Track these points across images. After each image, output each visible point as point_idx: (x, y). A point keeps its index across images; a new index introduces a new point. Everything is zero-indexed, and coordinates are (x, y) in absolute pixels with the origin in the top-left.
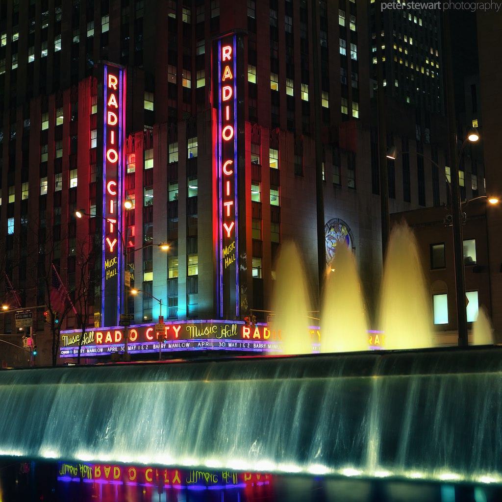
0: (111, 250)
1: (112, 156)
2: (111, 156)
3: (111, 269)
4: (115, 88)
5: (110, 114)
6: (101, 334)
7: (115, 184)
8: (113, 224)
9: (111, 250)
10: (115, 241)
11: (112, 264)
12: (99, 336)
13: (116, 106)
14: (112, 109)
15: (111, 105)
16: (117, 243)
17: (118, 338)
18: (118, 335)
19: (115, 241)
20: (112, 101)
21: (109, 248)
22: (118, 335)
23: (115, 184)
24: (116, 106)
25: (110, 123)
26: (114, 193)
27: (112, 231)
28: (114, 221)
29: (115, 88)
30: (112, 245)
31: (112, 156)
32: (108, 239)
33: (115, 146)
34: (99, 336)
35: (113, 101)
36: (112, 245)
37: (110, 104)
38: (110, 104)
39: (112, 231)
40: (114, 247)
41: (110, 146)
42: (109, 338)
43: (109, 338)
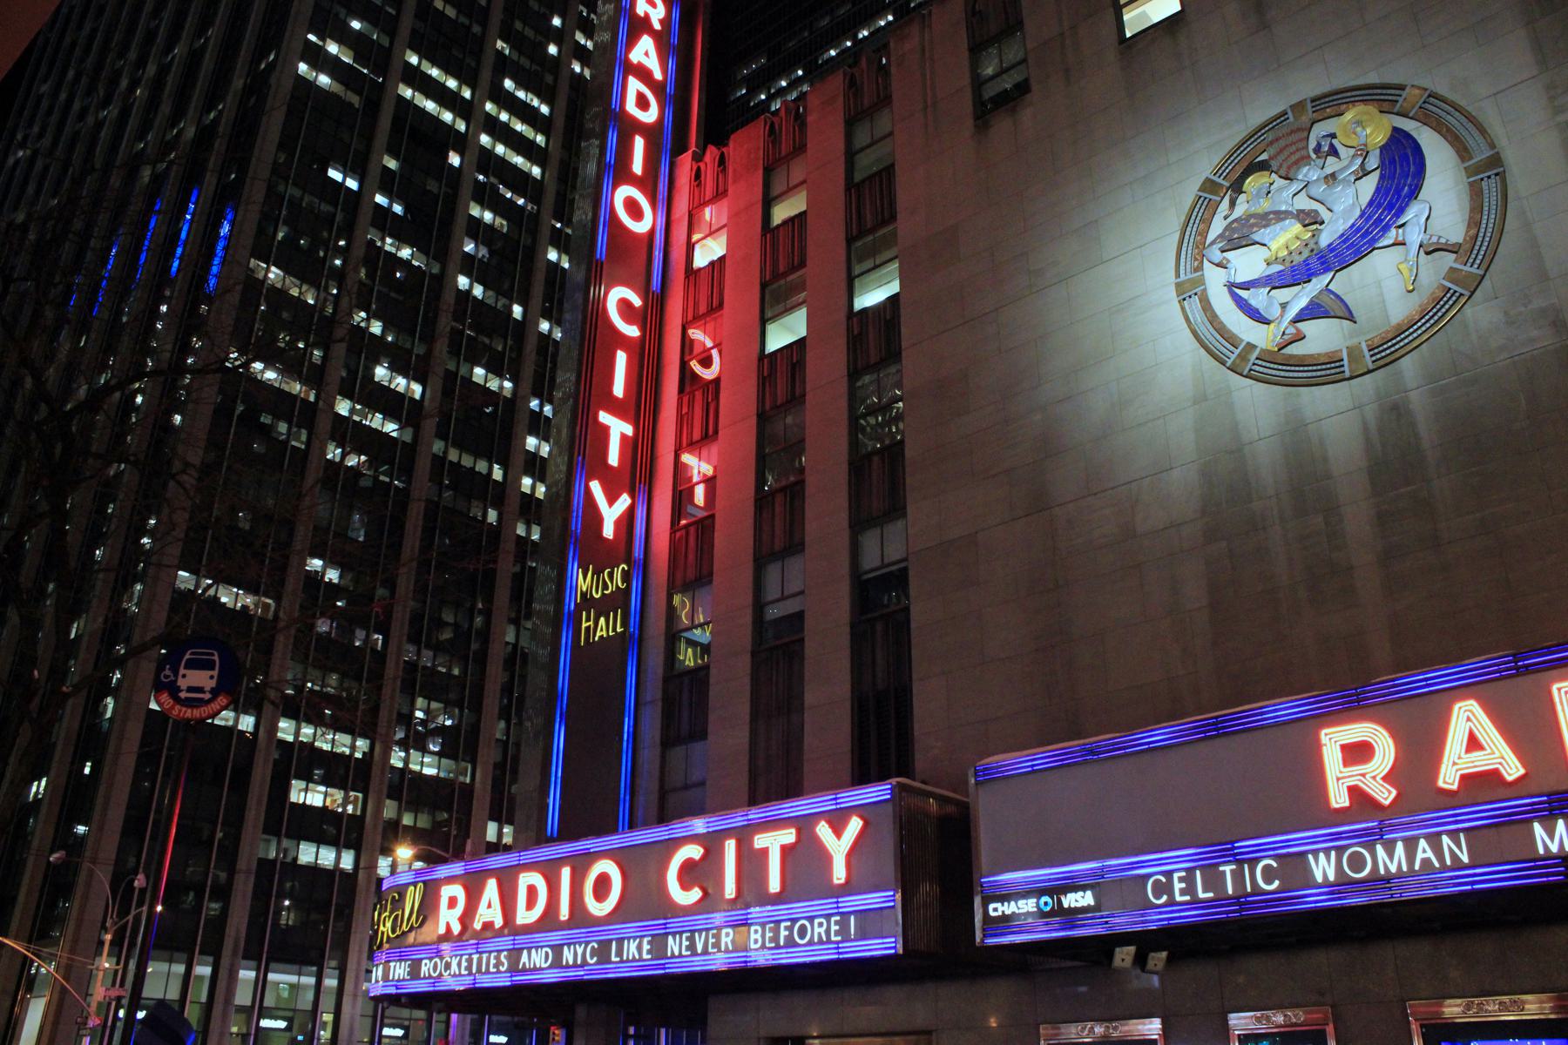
0: (608, 531)
1: (633, 208)
2: (631, 209)
3: (603, 607)
4: (657, 26)
5: (634, 85)
6: (457, 890)
7: (637, 301)
8: (623, 436)
9: (608, 531)
10: (624, 501)
11: (605, 587)
12: (452, 902)
13: (658, 75)
14: (643, 74)
15: (640, 65)
16: (630, 512)
17: (531, 904)
18: (532, 890)
19: (624, 501)
20: (644, 52)
21: (598, 520)
22: (532, 890)
23: (637, 301)
24: (658, 75)
25: (631, 107)
26: (632, 331)
27: (613, 458)
28: (629, 430)
29: (657, 26)
30: (611, 514)
31: (633, 208)
32: (596, 487)
33: (647, 183)
34: (452, 902)
35: (646, 54)
36: (611, 514)
37: (636, 56)
38: (636, 56)
39: (613, 458)
40: (617, 523)
41: (622, 174)
42: (489, 910)
43: (489, 910)
